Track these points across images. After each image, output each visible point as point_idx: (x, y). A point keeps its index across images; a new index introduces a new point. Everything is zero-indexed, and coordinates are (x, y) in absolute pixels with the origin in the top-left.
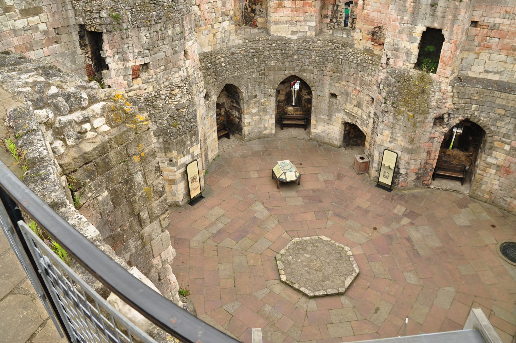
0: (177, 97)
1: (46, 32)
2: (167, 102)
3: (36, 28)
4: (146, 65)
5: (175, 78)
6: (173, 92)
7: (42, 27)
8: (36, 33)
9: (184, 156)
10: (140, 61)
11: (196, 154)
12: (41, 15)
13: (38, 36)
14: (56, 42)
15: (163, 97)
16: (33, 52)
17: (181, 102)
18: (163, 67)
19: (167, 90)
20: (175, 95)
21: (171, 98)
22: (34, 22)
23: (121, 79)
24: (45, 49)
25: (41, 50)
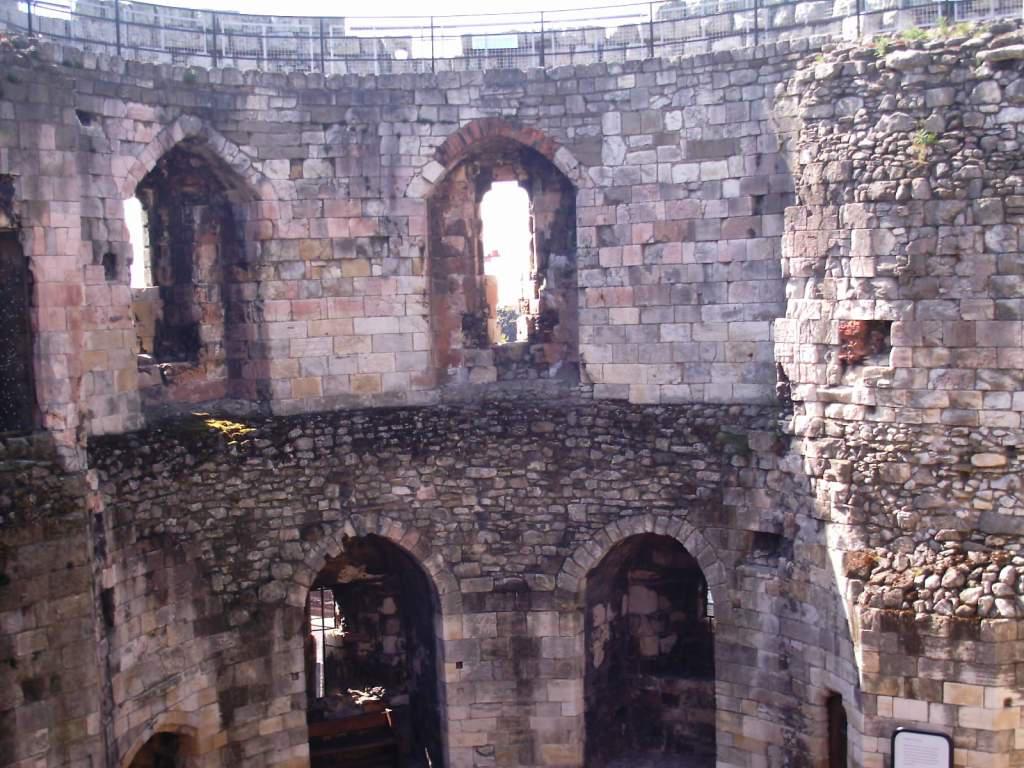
0: (994, 485)
1: (732, 203)
2: (943, 484)
3: (713, 188)
4: (884, 326)
5: (994, 409)
6: (976, 460)
7: (732, 189)
8: (711, 202)
9: (911, 695)
10: (862, 312)
11: (969, 718)
12: (732, 158)
13: (714, 208)
14: (752, 234)
15: (925, 458)
16: (692, 244)
17: (1001, 511)
18: (941, 351)
19: (953, 444)
20: (987, 473)
21: (965, 477)
22: (714, 172)
23: (809, 353)
24: (722, 244)
25: (712, 245)
